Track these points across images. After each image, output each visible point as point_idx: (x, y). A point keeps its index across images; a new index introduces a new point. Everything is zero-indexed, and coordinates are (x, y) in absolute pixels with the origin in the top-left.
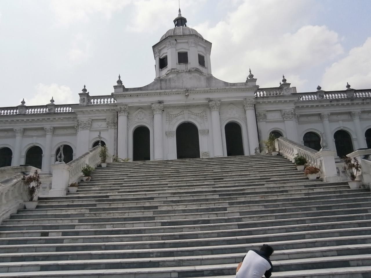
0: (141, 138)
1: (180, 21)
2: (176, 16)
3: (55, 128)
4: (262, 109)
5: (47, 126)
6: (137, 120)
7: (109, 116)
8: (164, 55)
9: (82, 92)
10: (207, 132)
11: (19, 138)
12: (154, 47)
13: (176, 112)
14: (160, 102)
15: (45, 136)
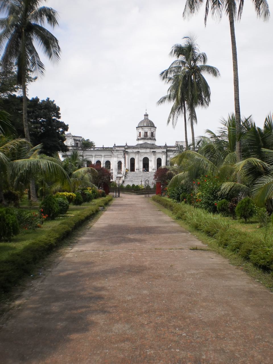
0: (132, 161)
1: (146, 115)
2: (145, 113)
3: (105, 155)
4: (169, 153)
5: (103, 154)
6: (131, 156)
7: (123, 154)
8: (140, 132)
9: (114, 145)
10: (151, 161)
11: (93, 158)
12: (137, 128)
13: (143, 154)
14: (139, 152)
15: (102, 157)
